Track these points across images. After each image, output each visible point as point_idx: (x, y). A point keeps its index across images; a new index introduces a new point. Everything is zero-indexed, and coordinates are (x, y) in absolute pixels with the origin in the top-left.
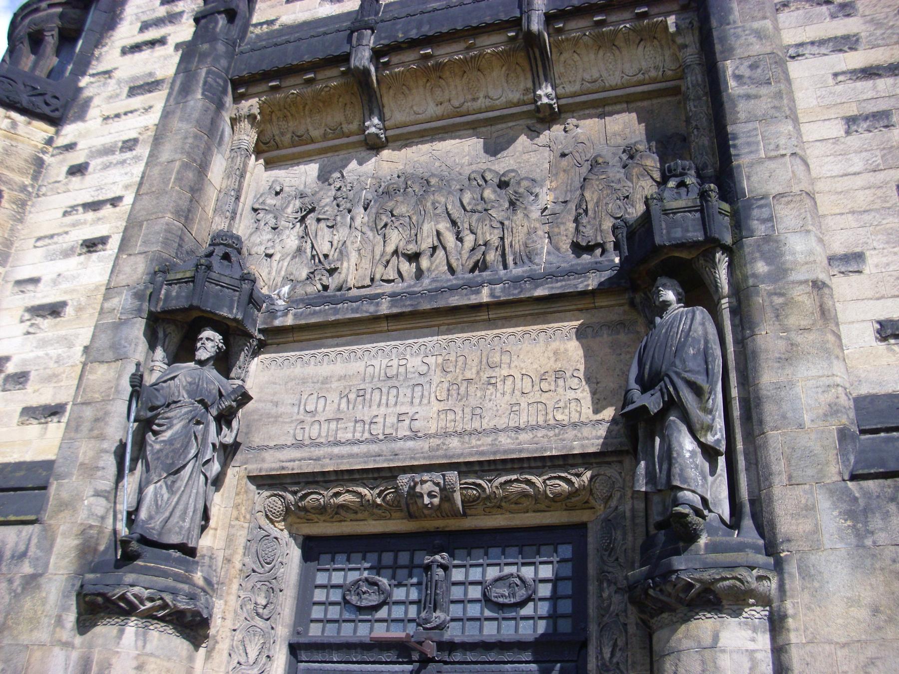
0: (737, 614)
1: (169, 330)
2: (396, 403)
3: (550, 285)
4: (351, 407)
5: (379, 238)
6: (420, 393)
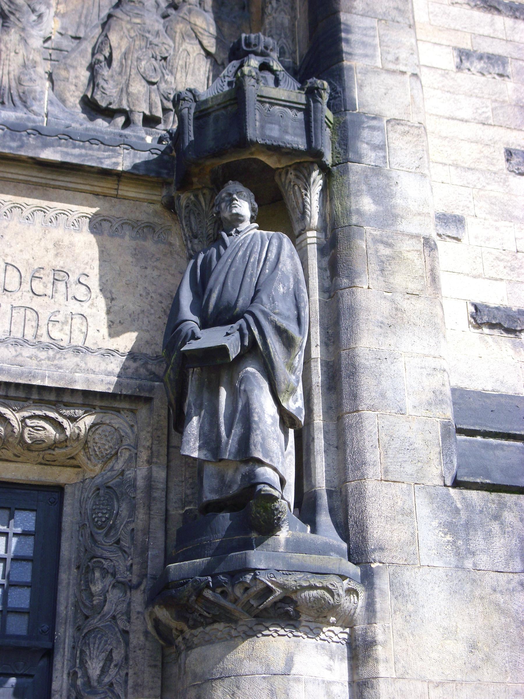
0: (314, 632)
3: (65, 150)
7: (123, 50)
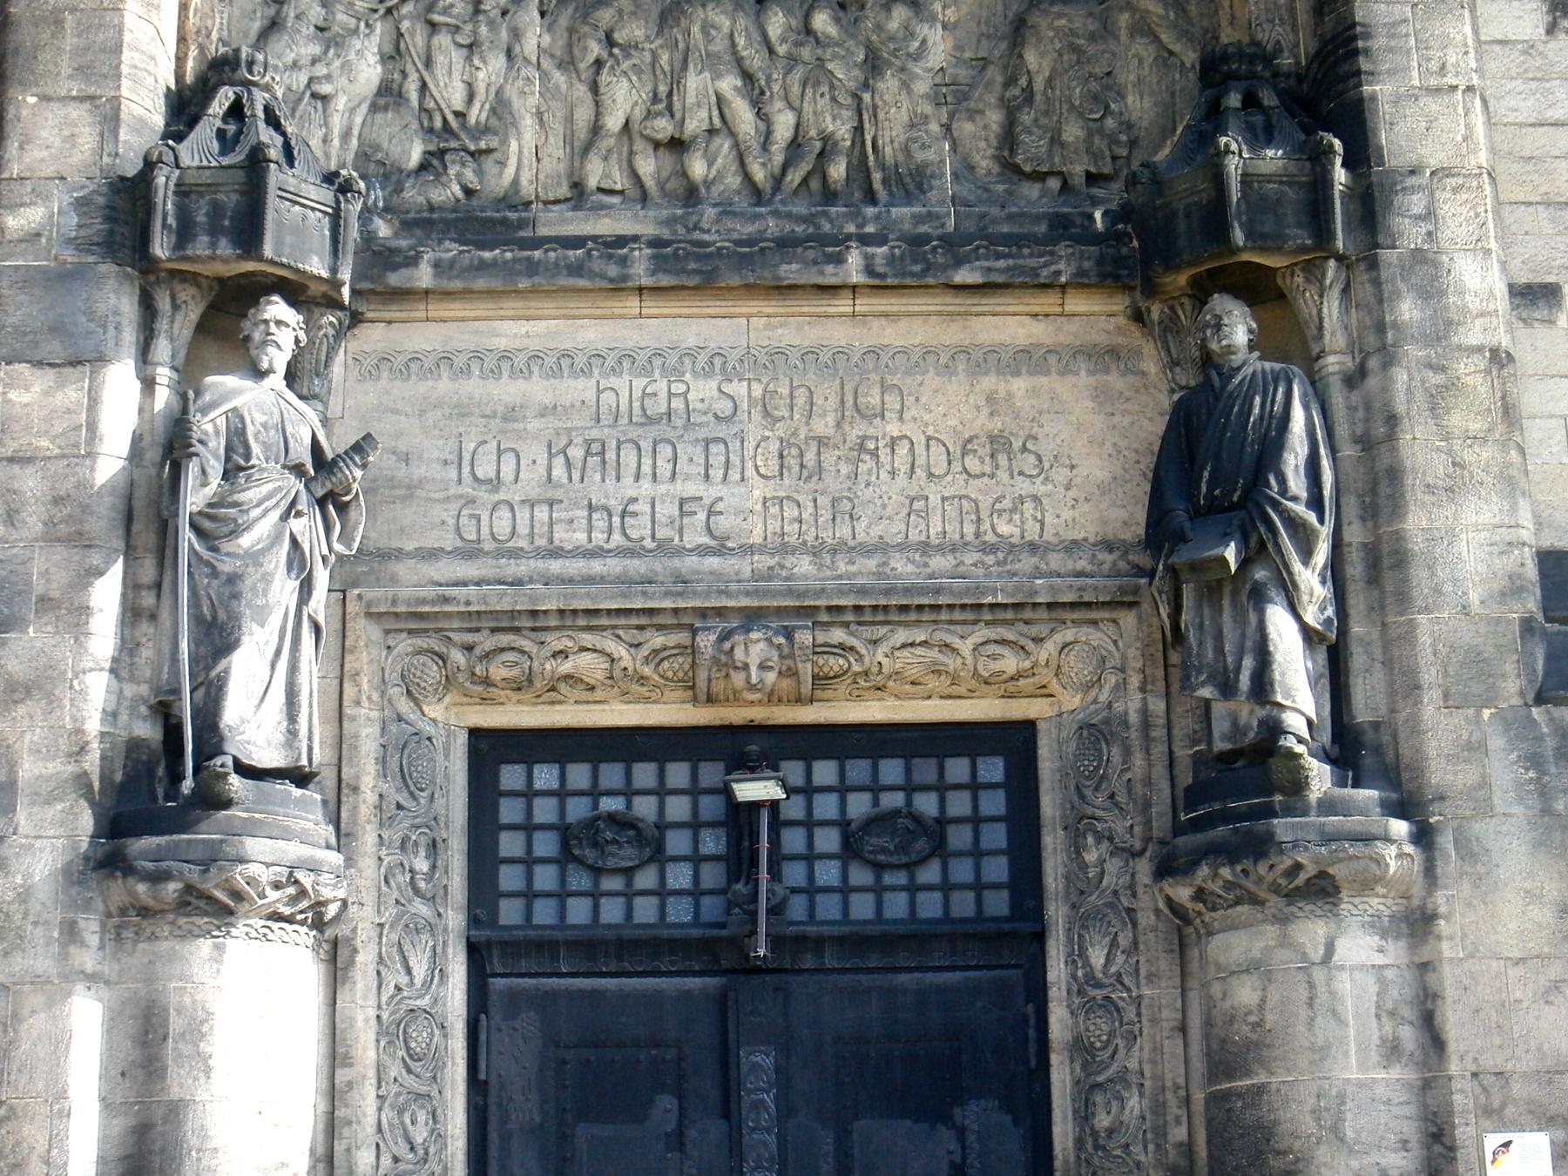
1: (182, 296)
2: (674, 473)
3: (986, 264)
4: (576, 476)
5: (581, 90)
6: (723, 459)
7: (1047, 74)
